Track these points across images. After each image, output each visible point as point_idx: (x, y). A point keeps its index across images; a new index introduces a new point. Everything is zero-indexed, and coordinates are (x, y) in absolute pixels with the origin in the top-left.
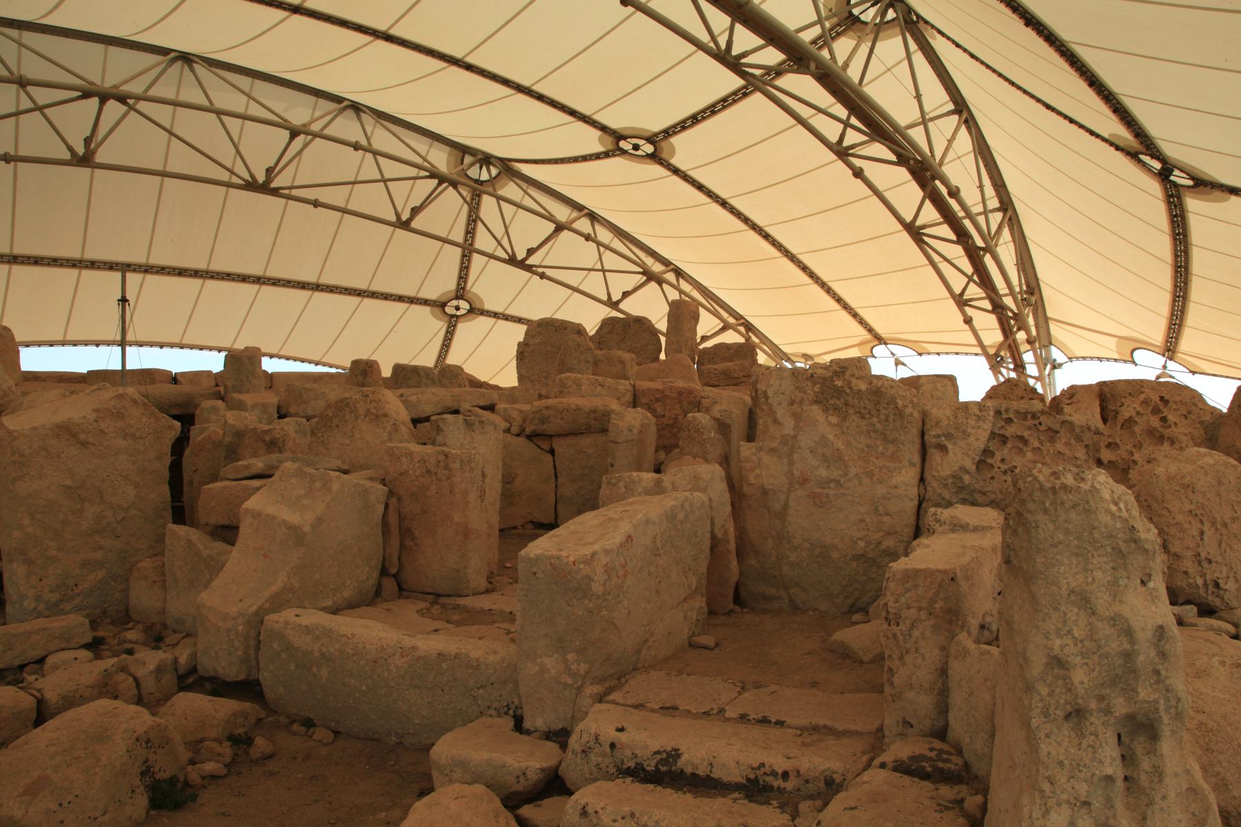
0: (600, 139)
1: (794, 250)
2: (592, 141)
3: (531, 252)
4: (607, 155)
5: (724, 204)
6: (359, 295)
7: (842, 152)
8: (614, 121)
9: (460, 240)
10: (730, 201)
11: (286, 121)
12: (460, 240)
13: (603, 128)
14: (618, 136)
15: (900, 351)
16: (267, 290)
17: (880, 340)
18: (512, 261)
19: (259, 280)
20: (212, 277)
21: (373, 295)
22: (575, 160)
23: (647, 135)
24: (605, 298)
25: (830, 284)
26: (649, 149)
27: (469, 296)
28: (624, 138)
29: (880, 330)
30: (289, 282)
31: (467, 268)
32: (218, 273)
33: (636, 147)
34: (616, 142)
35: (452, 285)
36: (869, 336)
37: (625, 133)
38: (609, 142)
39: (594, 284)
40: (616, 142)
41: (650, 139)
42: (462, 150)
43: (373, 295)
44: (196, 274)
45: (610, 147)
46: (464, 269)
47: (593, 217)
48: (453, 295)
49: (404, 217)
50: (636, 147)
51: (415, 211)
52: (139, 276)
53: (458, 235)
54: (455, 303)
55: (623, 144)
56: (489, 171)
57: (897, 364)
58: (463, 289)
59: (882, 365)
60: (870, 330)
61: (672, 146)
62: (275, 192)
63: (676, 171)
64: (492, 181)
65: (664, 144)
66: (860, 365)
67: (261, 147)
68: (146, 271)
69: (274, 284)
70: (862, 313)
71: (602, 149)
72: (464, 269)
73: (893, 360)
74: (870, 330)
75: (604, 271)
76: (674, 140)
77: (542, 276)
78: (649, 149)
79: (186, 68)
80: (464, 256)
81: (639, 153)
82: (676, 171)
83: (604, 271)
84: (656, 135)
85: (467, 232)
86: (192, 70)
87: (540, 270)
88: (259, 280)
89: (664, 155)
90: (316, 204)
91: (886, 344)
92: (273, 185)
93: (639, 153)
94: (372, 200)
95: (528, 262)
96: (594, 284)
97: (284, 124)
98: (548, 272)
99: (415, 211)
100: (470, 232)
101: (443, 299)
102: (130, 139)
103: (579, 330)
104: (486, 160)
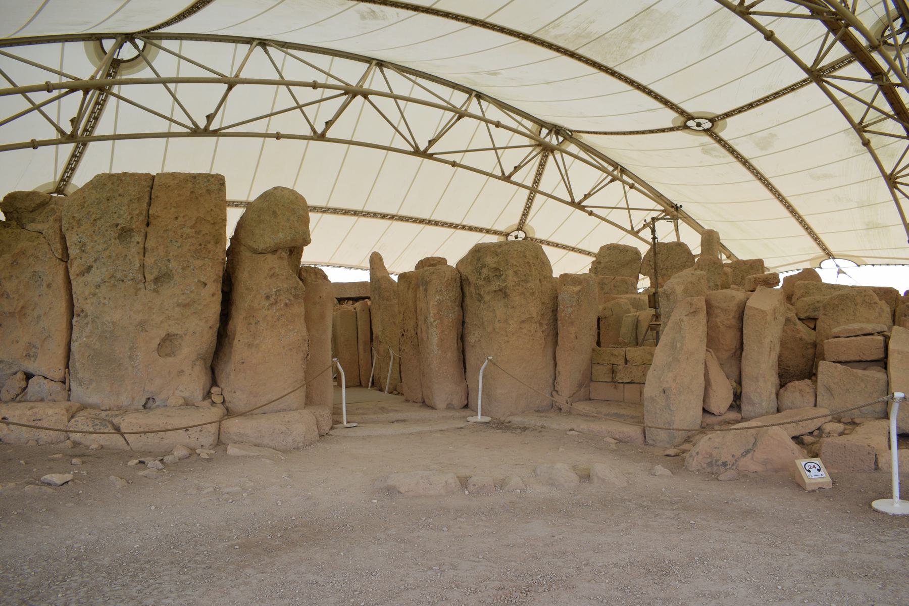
0: (673, 121)
1: (784, 193)
2: (669, 118)
3: (586, 197)
4: (672, 129)
5: (745, 162)
6: (454, 227)
7: (860, 128)
8: (689, 108)
9: (530, 185)
10: (750, 161)
11: (454, 107)
12: (530, 185)
13: (682, 112)
14: (690, 117)
15: (843, 264)
16: (397, 224)
17: (830, 255)
18: (573, 203)
19: (393, 217)
20: (364, 216)
21: (464, 227)
22: (644, 132)
23: (711, 116)
24: (629, 228)
25: (804, 217)
26: (709, 125)
27: (526, 228)
28: (693, 118)
29: (832, 248)
30: (412, 218)
31: (529, 208)
32: (368, 213)
33: (699, 125)
34: (686, 120)
35: (516, 221)
36: (820, 252)
37: (695, 115)
38: (680, 120)
39: (621, 217)
40: (686, 120)
41: (712, 120)
42: (542, 124)
43: (464, 227)
44: (355, 213)
45: (679, 124)
46: (528, 208)
47: (623, 171)
48: (516, 227)
49: (507, 174)
50: (699, 125)
51: (517, 169)
52: (318, 215)
53: (529, 183)
54: (516, 233)
55: (691, 123)
56: (557, 139)
57: (838, 273)
58: (523, 223)
59: (828, 274)
60: (825, 249)
61: (726, 125)
62: (431, 156)
63: (720, 141)
64: (560, 144)
65: (720, 123)
66: (810, 275)
67: (425, 123)
68: (324, 212)
69: (402, 220)
70: (822, 237)
71: (671, 126)
72: (528, 208)
73: (837, 270)
74: (825, 249)
75: (628, 209)
76: (728, 120)
77: (591, 213)
78: (709, 125)
79: (378, 69)
80: (529, 199)
81: (701, 128)
82: (720, 141)
83: (628, 209)
84: (718, 117)
85: (535, 182)
86: (382, 72)
87: (589, 209)
88: (393, 217)
89: (716, 130)
90: (454, 164)
91: (834, 258)
92: (429, 152)
93: (701, 128)
94: (487, 161)
95: (583, 204)
96: (621, 217)
97: (453, 109)
98: (595, 211)
99: (517, 169)
100: (537, 181)
101: (508, 231)
102: (360, 120)
103: (636, 252)
104: (557, 130)
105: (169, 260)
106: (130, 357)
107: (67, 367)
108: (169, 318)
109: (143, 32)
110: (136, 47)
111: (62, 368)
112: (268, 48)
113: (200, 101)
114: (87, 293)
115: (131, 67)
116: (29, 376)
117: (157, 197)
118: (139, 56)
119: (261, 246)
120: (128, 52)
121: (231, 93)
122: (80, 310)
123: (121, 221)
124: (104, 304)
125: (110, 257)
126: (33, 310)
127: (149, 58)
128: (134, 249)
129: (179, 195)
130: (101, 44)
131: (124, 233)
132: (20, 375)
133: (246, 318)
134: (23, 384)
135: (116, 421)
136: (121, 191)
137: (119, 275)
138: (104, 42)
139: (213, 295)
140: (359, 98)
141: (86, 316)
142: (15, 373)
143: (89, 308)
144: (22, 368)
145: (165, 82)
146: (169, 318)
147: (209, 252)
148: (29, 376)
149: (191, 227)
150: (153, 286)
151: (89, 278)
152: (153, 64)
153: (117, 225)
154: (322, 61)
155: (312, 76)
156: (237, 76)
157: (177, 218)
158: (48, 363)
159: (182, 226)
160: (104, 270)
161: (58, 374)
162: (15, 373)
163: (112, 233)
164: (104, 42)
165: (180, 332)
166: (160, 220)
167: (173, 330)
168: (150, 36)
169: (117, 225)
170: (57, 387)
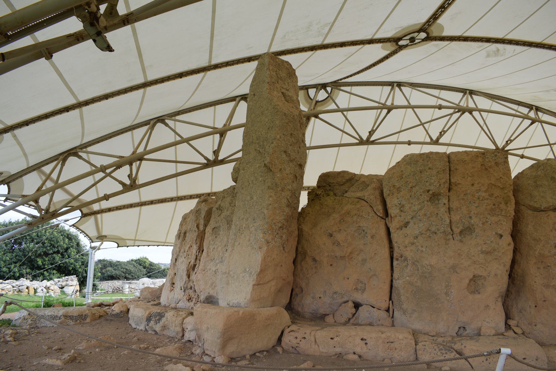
105: (470, 217)
106: (446, 293)
107: (390, 299)
108: (474, 262)
109: (331, 83)
110: (327, 92)
111: (388, 300)
112: (402, 88)
113: (363, 122)
114: (407, 242)
115: (323, 105)
116: (357, 306)
117: (456, 169)
118: (328, 97)
119: (544, 206)
120: (322, 95)
121: (389, 115)
122: (399, 255)
123: (432, 188)
124: (422, 251)
125: (425, 215)
126: (358, 255)
127: (334, 98)
128: (443, 209)
129: (473, 168)
130: (308, 92)
131: (434, 197)
132: (351, 304)
133: (535, 263)
134: (354, 310)
135: (457, 346)
136: (430, 165)
137: (433, 229)
138: (310, 90)
139: (509, 245)
140: (467, 114)
141: (406, 259)
142: (347, 302)
143: (408, 254)
144: (352, 298)
145: (342, 111)
146: (474, 262)
147: (502, 210)
148: (357, 306)
149: (485, 192)
150: (459, 238)
151: (407, 231)
152: (336, 101)
153: (428, 191)
154: (435, 92)
155: (433, 101)
156: (392, 104)
157: (473, 185)
158: (375, 295)
159: (478, 191)
160: (421, 225)
161: (384, 304)
162: (347, 302)
163: (426, 197)
164: (310, 90)
165: (484, 274)
166: (460, 186)
167: (479, 272)
168: (337, 85)
169: (428, 191)
170: (384, 314)
